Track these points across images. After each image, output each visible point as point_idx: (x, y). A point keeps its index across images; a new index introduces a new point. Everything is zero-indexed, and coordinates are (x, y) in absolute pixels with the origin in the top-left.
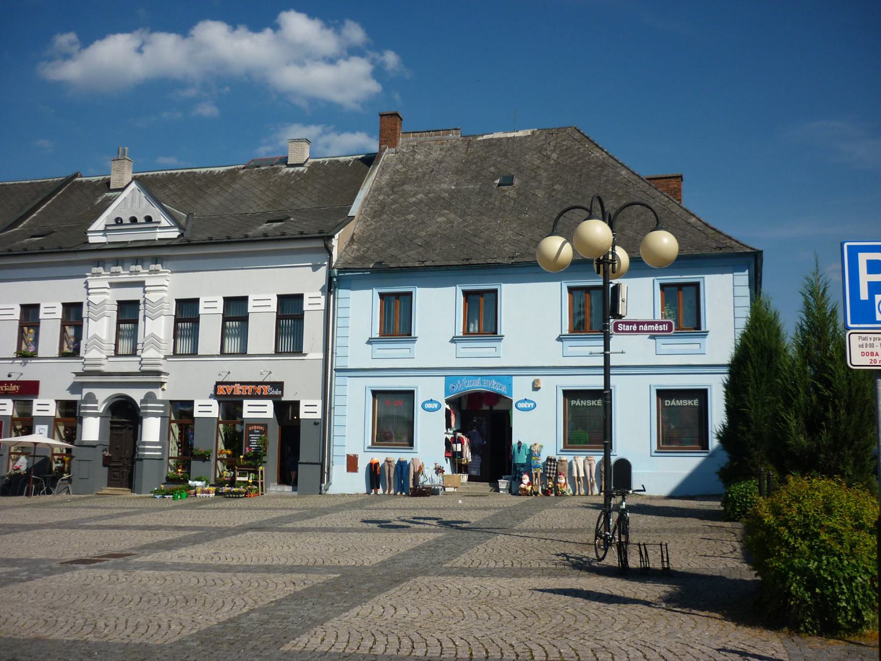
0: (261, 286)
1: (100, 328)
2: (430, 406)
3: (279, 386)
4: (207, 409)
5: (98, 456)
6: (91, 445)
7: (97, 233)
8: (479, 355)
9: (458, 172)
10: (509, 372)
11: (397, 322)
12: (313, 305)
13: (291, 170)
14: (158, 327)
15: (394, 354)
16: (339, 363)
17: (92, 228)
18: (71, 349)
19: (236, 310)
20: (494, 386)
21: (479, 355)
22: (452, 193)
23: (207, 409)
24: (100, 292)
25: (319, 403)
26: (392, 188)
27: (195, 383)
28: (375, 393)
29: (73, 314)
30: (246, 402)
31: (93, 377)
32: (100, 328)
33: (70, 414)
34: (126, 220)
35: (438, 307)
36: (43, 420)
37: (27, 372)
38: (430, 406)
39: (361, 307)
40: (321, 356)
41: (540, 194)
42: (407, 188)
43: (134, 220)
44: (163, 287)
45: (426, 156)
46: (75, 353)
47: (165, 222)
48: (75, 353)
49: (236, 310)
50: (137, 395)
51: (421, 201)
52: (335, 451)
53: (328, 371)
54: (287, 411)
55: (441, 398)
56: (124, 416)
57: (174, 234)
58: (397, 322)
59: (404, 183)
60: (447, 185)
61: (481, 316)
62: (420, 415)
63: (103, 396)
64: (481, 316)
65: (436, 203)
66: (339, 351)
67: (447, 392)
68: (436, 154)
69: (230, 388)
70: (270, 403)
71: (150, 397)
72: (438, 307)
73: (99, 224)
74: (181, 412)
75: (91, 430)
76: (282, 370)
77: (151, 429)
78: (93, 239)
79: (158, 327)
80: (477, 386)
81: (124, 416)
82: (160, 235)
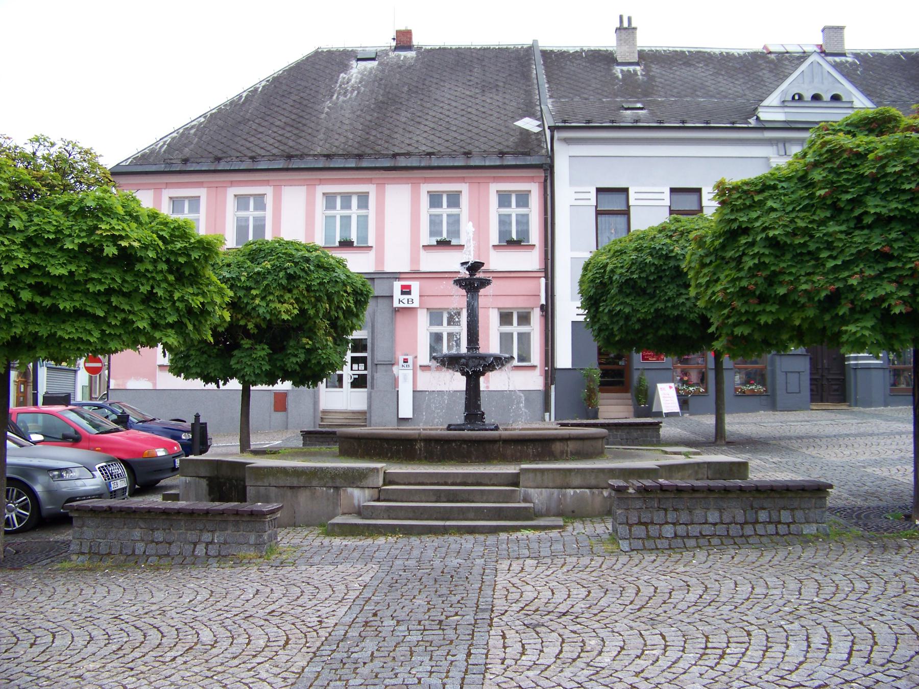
17: (765, 103)
34: (827, 97)
43: (816, 98)
73: (774, 99)
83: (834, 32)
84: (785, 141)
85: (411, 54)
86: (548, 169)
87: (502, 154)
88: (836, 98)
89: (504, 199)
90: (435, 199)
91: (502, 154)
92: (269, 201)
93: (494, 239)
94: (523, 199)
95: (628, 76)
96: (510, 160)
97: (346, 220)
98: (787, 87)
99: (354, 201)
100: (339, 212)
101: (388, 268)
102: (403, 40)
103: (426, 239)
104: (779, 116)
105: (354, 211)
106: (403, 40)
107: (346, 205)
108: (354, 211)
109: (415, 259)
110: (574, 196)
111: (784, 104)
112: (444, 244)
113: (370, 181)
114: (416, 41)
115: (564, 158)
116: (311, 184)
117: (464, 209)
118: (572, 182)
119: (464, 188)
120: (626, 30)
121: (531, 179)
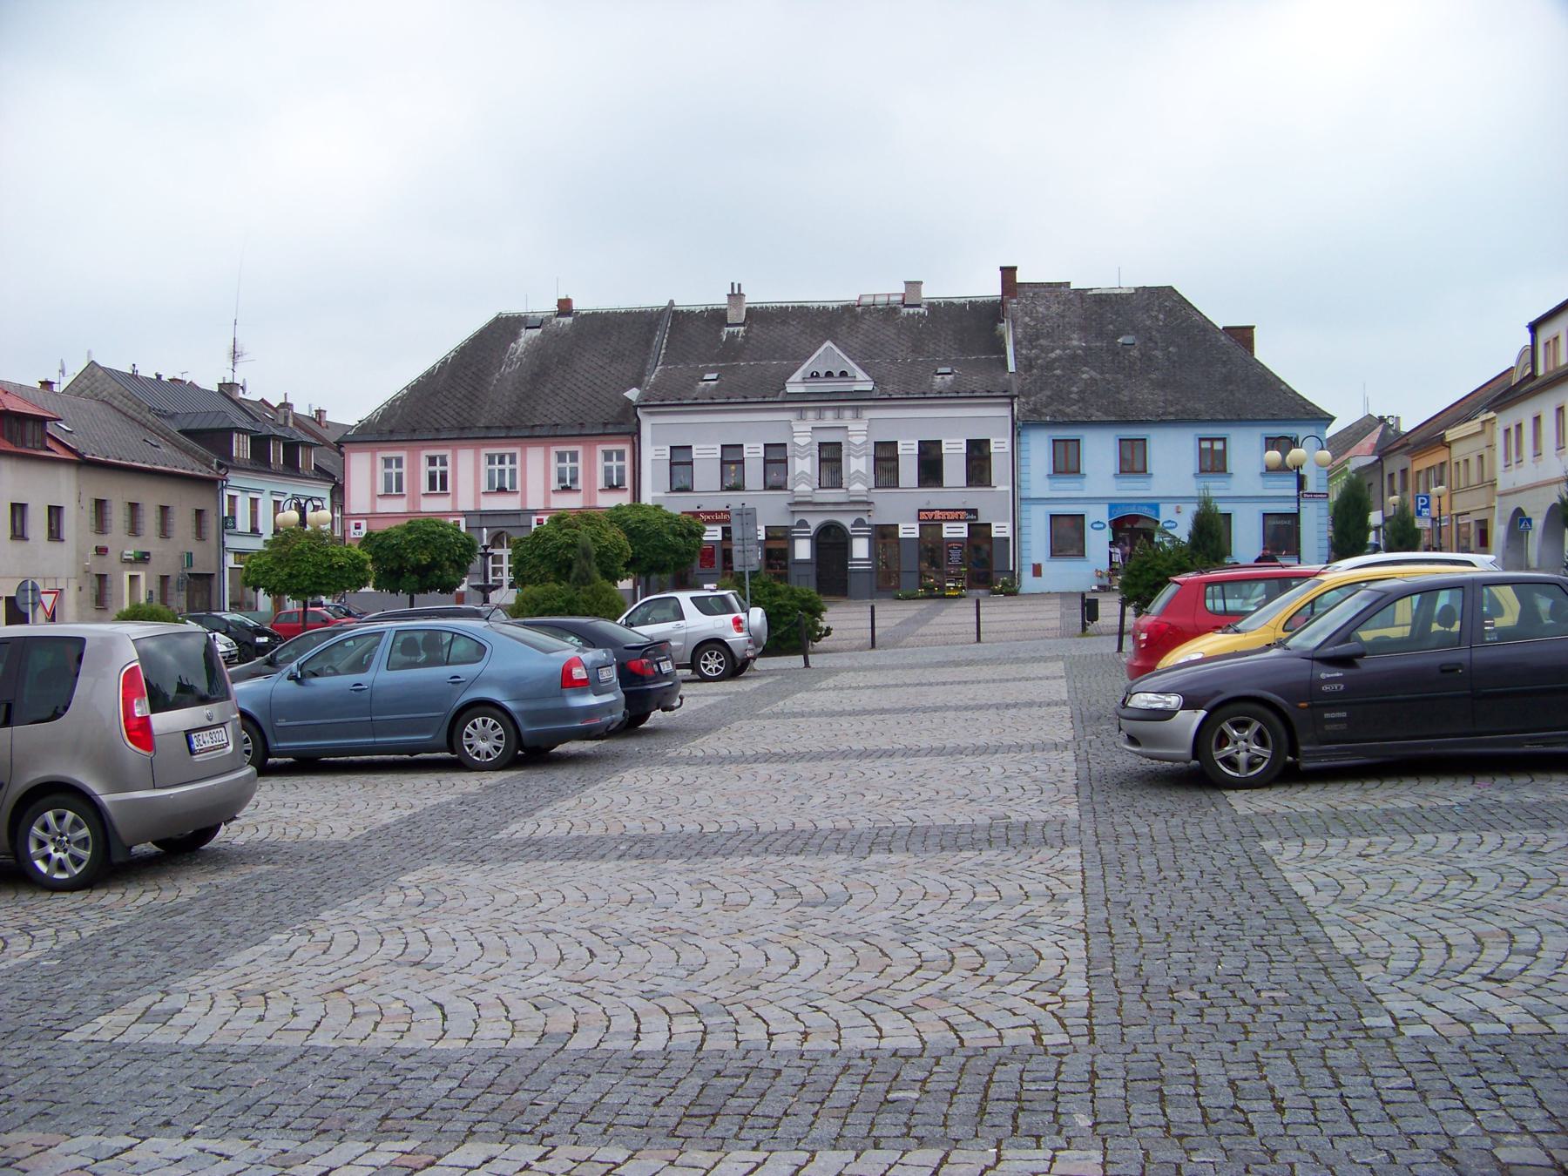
1: (804, 466)
2: (1098, 526)
3: (974, 512)
4: (909, 530)
5: (812, 571)
6: (803, 562)
7: (795, 385)
8: (1133, 489)
9: (1082, 328)
11: (1067, 463)
12: (1000, 447)
13: (911, 311)
14: (858, 465)
15: (1067, 487)
16: (1024, 494)
18: (775, 485)
20: (1145, 512)
23: (909, 530)
24: (802, 434)
25: (1009, 525)
26: (1030, 342)
27: (903, 510)
28: (1052, 516)
29: (776, 456)
30: (945, 525)
31: (797, 505)
32: (804, 466)
35: (1100, 450)
37: (734, 500)
38: (1098, 526)
39: (1039, 448)
40: (1010, 488)
41: (1158, 353)
43: (829, 374)
45: (1048, 308)
46: (781, 487)
47: (861, 375)
50: (847, 521)
51: (1058, 359)
52: (1024, 561)
53: (1018, 501)
54: (979, 531)
55: (1106, 520)
56: (831, 541)
58: (1067, 463)
59: (1038, 338)
62: (1090, 534)
63: (815, 522)
66: (1023, 485)
67: (1110, 515)
68: (1055, 308)
69: (930, 514)
70: (965, 525)
71: (859, 523)
72: (1100, 450)
73: (797, 376)
74: (884, 535)
75: (803, 550)
77: (860, 549)
78: (789, 390)
79: (858, 465)
80: (1132, 511)
81: (831, 541)
83: (914, 286)
84: (801, 409)
85: (569, 320)
86: (635, 435)
87: (605, 424)
88: (843, 374)
89: (608, 456)
90: (561, 457)
91: (605, 424)
92: (449, 460)
93: (601, 484)
94: (621, 456)
95: (732, 336)
96: (610, 429)
97: (502, 472)
98: (806, 367)
99: (507, 459)
100: (497, 467)
101: (530, 507)
102: (565, 307)
103: (555, 485)
104: (801, 389)
106: (565, 307)
107: (501, 462)
108: (507, 466)
109: (547, 500)
110: (654, 454)
111: (804, 380)
112: (566, 489)
113: (515, 445)
114: (576, 306)
115: (648, 425)
116: (477, 449)
117: (580, 465)
118: (654, 442)
119: (579, 449)
120: (736, 296)
121: (624, 442)
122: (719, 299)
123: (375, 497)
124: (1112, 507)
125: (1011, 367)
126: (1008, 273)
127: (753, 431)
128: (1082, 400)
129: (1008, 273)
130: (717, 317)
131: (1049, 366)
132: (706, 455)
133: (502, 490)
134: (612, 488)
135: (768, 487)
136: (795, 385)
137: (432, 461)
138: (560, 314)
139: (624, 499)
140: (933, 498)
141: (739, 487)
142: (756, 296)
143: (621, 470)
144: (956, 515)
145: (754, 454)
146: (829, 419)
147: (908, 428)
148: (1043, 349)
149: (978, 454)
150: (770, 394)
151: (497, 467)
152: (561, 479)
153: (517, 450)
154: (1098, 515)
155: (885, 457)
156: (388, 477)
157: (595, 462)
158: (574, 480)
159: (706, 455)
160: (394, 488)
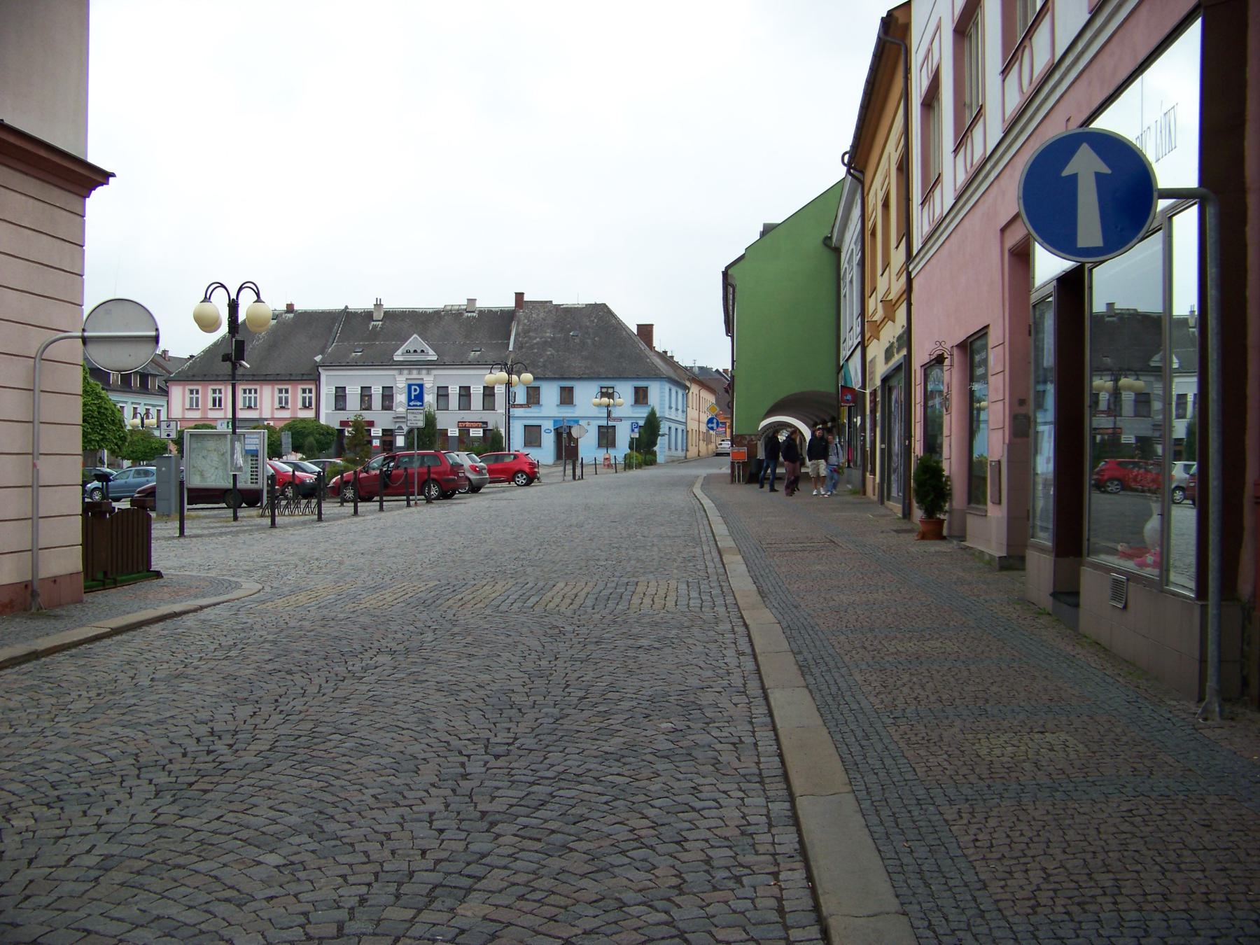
0: (477, 380)
1: (400, 398)
3: (486, 423)
7: (398, 357)
8: (566, 412)
9: (554, 327)
10: (576, 421)
12: (500, 390)
19: (465, 392)
21: (566, 412)
22: (553, 339)
24: (400, 382)
32: (400, 398)
33: (388, 434)
35: (550, 393)
36: (376, 437)
37: (367, 416)
41: (589, 341)
42: (531, 334)
44: (430, 381)
46: (390, 408)
47: (431, 352)
48: (390, 408)
49: (465, 392)
57: (435, 358)
60: (549, 334)
61: (567, 397)
62: (544, 435)
64: (567, 397)
65: (545, 344)
68: (542, 315)
72: (550, 393)
73: (399, 352)
76: (488, 417)
82: (429, 358)
85: (291, 315)
86: (317, 380)
90: (280, 391)
94: (310, 391)
95: (375, 327)
101: (264, 416)
102: (290, 308)
103: (277, 405)
104: (401, 359)
105: (253, 395)
106: (290, 308)
108: (253, 395)
110: (327, 391)
112: (282, 408)
114: (296, 308)
115: (324, 375)
117: (289, 395)
122: (369, 305)
123: (185, 409)
124: (555, 422)
125: (511, 348)
126: (519, 296)
127: (376, 380)
128: (544, 366)
129: (519, 296)
130: (368, 315)
131: (532, 347)
132: (353, 393)
133: (250, 407)
134: (305, 407)
135: (384, 408)
136: (398, 357)
137: (214, 391)
138: (287, 312)
139: (310, 414)
140: (467, 416)
141: (369, 408)
142: (389, 304)
143: (310, 398)
144: (477, 424)
145: (377, 392)
146: (415, 375)
147: (454, 379)
148: (530, 338)
149: (489, 392)
150: (386, 362)
151: (248, 395)
152: (280, 402)
153: (258, 387)
154: (548, 425)
155: (442, 393)
156: (191, 399)
157: (296, 394)
158: (287, 403)
159: (353, 393)
160: (194, 405)
